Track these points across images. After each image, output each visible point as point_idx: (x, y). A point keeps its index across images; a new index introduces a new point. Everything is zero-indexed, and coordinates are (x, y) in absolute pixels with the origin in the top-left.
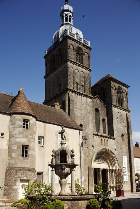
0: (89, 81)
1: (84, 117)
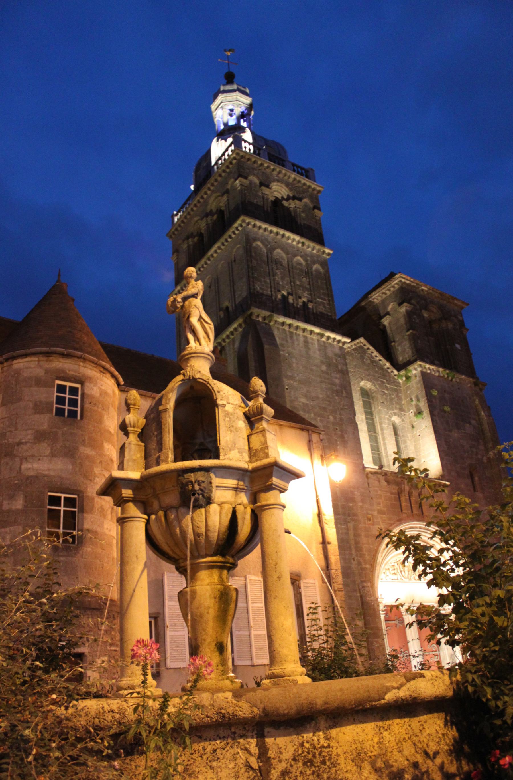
0: (325, 287)
1: (324, 409)
